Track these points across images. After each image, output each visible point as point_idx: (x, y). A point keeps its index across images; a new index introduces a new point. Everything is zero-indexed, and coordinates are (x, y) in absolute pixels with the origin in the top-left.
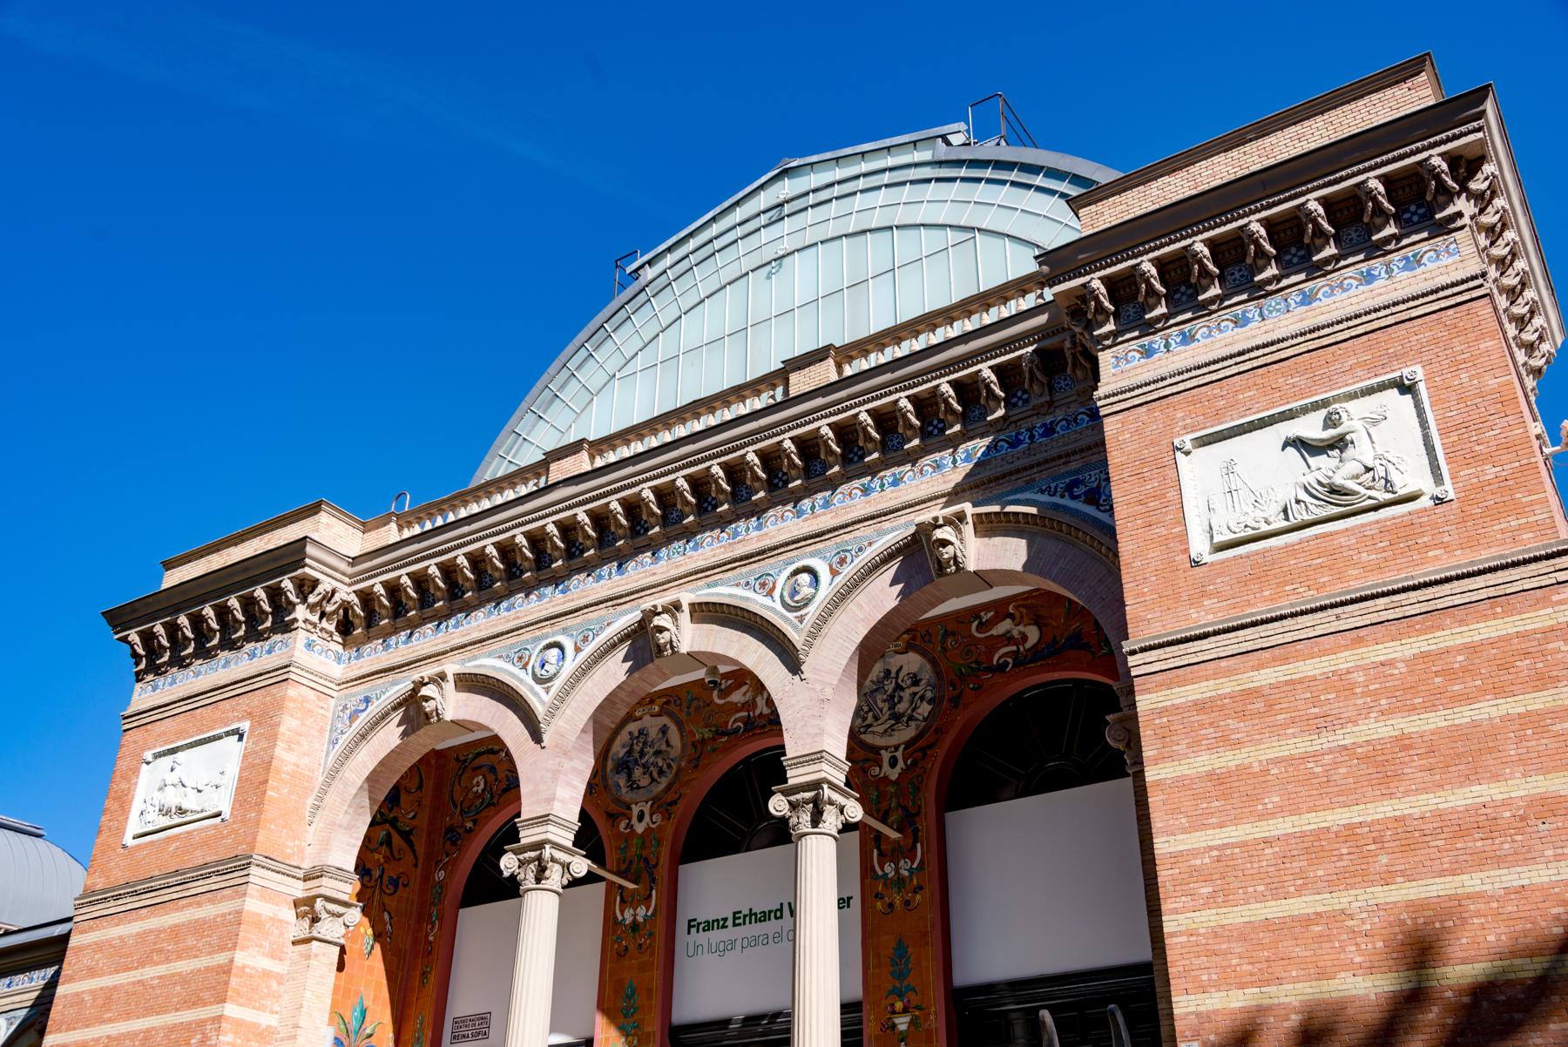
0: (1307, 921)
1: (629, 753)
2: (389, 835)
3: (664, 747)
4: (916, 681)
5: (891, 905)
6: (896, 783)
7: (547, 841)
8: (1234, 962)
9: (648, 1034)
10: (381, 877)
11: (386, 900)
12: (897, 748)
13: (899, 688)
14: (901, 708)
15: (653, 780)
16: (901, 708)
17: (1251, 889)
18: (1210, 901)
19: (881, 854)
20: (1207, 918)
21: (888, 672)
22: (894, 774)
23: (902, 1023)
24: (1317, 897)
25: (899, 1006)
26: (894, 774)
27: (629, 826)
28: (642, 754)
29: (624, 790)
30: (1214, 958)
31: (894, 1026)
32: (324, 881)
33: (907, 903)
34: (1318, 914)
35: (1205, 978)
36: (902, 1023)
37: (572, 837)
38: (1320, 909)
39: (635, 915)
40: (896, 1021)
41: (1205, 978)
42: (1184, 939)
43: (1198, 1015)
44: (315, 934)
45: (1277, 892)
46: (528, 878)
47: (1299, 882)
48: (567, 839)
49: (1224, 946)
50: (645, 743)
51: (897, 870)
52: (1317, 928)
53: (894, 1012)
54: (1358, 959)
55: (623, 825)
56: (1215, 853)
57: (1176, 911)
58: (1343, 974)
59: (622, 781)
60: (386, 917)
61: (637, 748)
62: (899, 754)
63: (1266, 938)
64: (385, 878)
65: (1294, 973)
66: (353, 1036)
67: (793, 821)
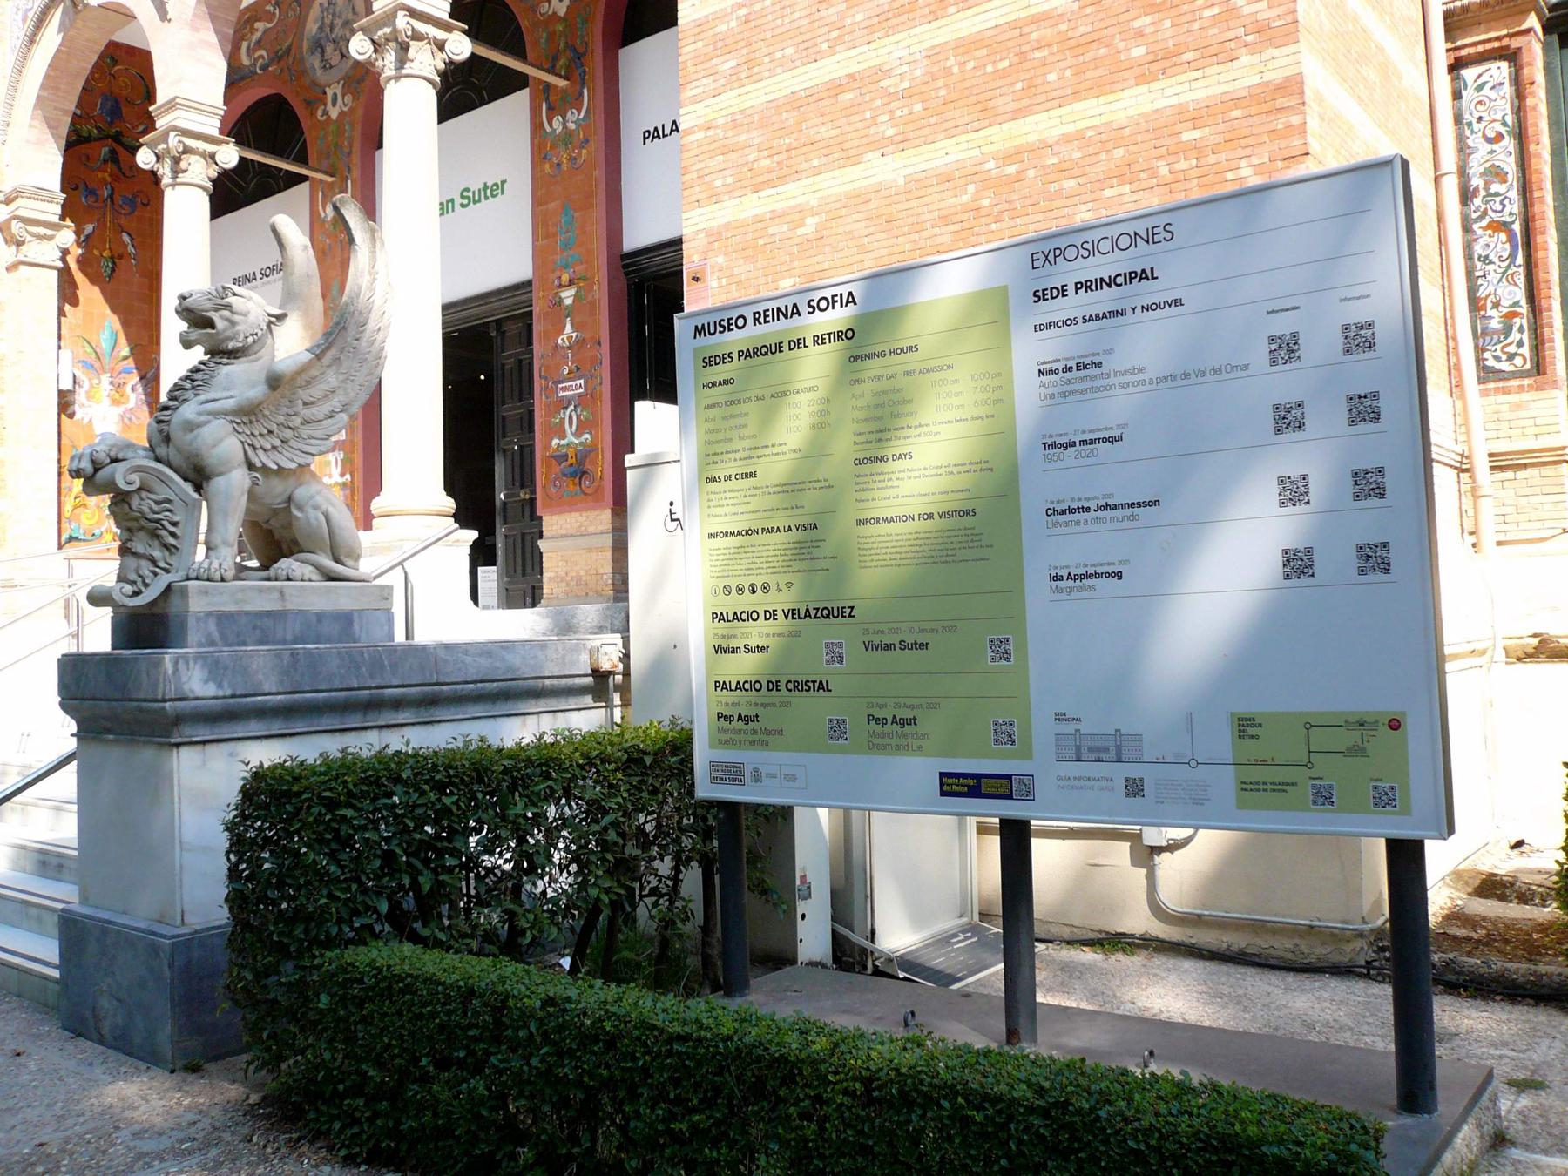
0: (835, 88)
1: (321, 28)
2: (113, 152)
3: (350, 16)
6: (565, 19)
7: (175, 128)
8: (752, 157)
10: (111, 196)
11: (123, 221)
17: (778, 55)
18: (734, 79)
19: (549, 108)
20: (732, 101)
23: (568, 296)
24: (852, 53)
25: (565, 278)
27: (326, 113)
28: (332, 28)
29: (319, 72)
30: (733, 156)
32: (19, 202)
33: (572, 160)
34: (852, 77)
35: (718, 183)
36: (568, 296)
37: (218, 124)
38: (854, 69)
40: (563, 295)
41: (718, 183)
42: (701, 135)
43: (708, 233)
44: (21, 257)
45: (810, 54)
46: (165, 171)
47: (835, 34)
48: (212, 127)
49: (743, 138)
50: (334, 14)
51: (564, 125)
52: (848, 96)
53: (561, 286)
54: (890, 132)
55: (319, 112)
56: (744, 11)
57: (695, 100)
58: (870, 155)
59: (315, 61)
60: (126, 238)
61: (328, 22)
63: (789, 118)
64: (116, 197)
65: (816, 163)
66: (106, 360)
67: (379, 63)
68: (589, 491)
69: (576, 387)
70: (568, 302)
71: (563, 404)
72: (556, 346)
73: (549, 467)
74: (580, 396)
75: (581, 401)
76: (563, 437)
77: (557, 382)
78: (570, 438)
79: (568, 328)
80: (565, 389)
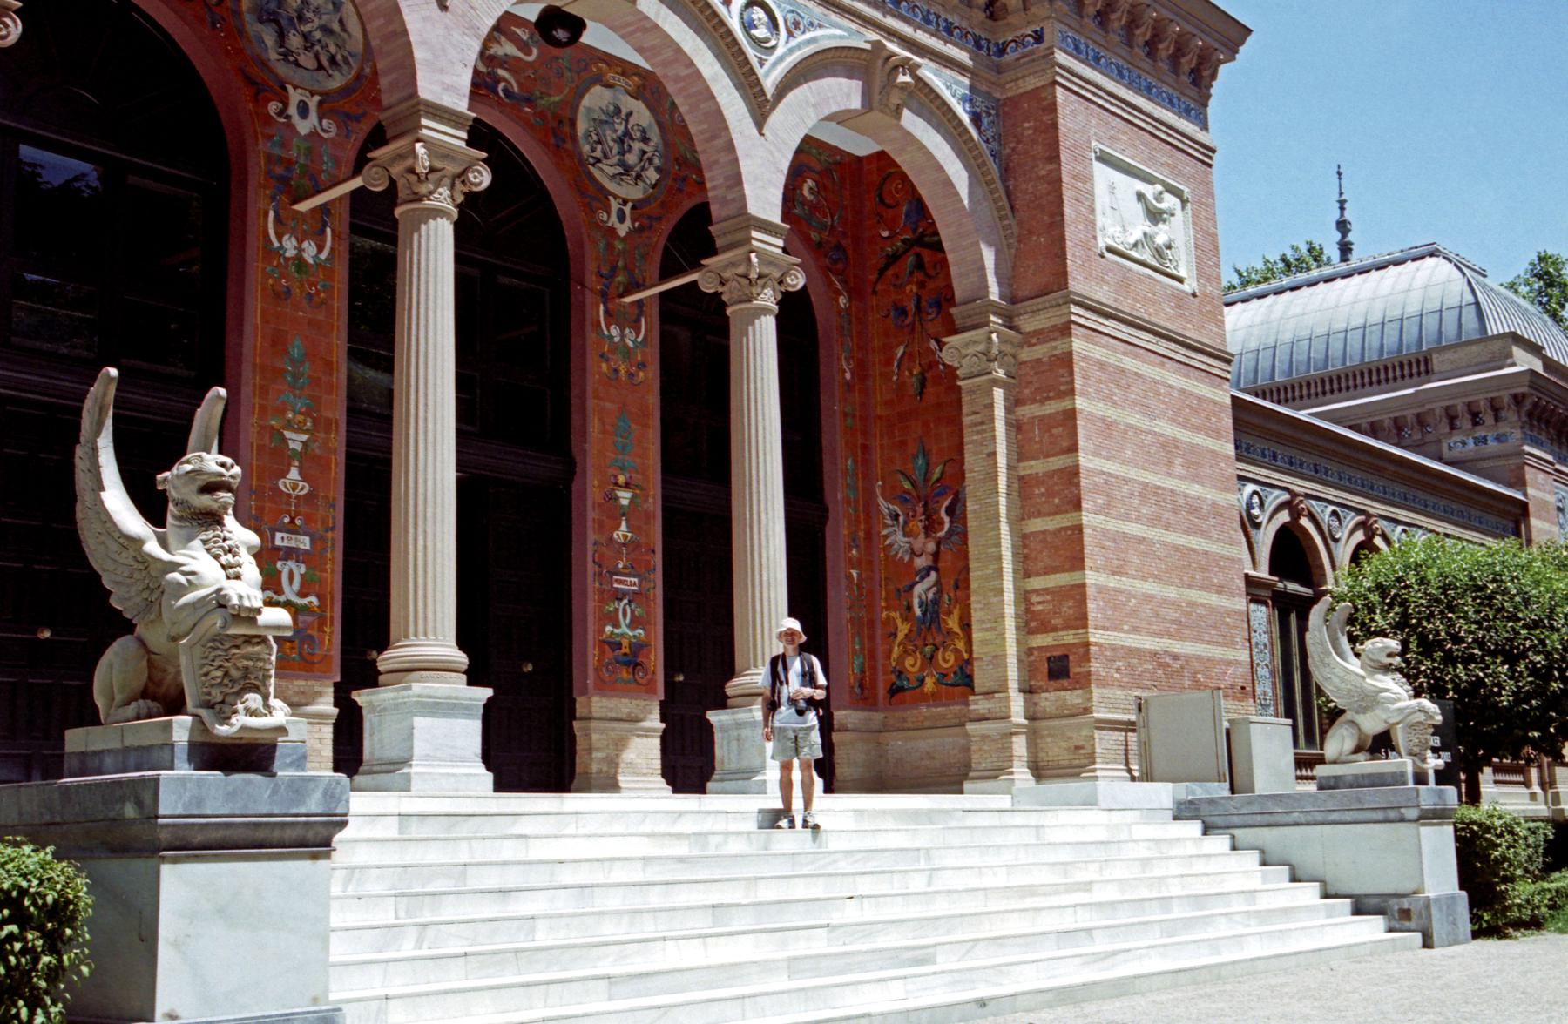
4: (645, 140)
5: (616, 371)
9: (328, 422)
12: (625, 202)
13: (627, 134)
14: (631, 159)
15: (320, 67)
16: (631, 159)
21: (618, 110)
22: (623, 230)
25: (621, 479)
26: (623, 230)
31: (617, 498)
36: (625, 497)
39: (300, 250)
55: (273, 107)
62: (627, 209)
68: (644, 681)
69: (630, 583)
70: (625, 502)
71: (618, 596)
72: (611, 538)
73: (602, 652)
74: (634, 592)
75: (635, 597)
76: (616, 625)
77: (612, 573)
78: (624, 629)
79: (624, 527)
80: (621, 582)
